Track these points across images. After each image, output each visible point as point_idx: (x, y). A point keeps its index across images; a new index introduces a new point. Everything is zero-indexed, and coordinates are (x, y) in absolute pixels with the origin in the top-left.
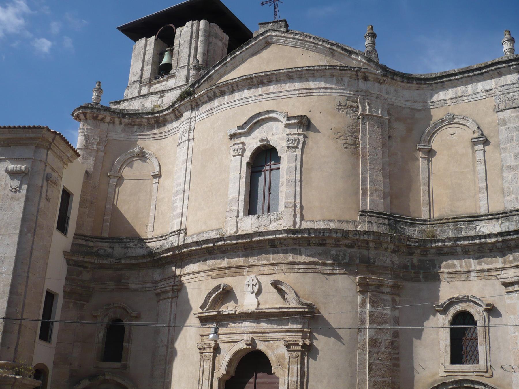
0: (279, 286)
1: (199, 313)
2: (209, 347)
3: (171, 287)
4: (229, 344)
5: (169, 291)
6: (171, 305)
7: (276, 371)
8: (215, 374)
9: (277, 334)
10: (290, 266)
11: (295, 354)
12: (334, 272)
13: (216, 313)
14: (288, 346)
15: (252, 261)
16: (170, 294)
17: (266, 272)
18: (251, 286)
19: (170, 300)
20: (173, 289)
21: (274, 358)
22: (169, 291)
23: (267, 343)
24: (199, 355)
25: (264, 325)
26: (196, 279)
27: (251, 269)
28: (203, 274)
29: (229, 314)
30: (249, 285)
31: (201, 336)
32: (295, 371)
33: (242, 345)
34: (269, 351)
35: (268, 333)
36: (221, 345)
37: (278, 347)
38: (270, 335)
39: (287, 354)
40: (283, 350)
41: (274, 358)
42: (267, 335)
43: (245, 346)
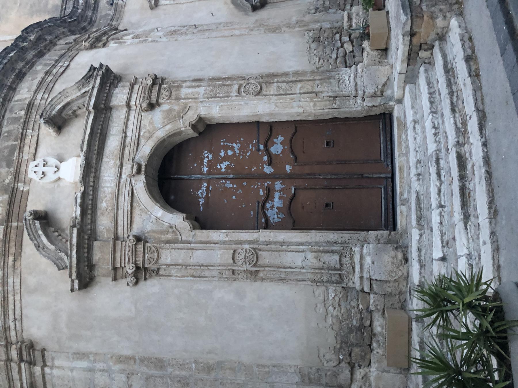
0: (54, 112)
1: (70, 276)
2: (135, 252)
3: (23, 365)
4: (136, 211)
5: (31, 375)
6: (58, 367)
7: (187, 123)
8: (184, 238)
9: (130, 122)
10: (33, 111)
11: (164, 93)
12: (66, 64)
13: (75, 231)
14: (151, 106)
15: (10, 177)
16: (37, 370)
17: (33, 150)
18: (45, 169)
19: (47, 370)
20: (27, 361)
21: (168, 127)
22: (31, 375)
23: (142, 141)
24: (149, 282)
25: (113, 143)
26: (18, 297)
27: (22, 177)
28: (10, 280)
29: (80, 206)
30: (43, 173)
31: (115, 279)
32: (190, 90)
33: (140, 183)
34: (155, 135)
35: (125, 137)
36: (135, 231)
37: (151, 123)
38: (129, 134)
39: (165, 107)
40: (158, 115)
41: (168, 127)
42: (128, 139)
43: (142, 177)
